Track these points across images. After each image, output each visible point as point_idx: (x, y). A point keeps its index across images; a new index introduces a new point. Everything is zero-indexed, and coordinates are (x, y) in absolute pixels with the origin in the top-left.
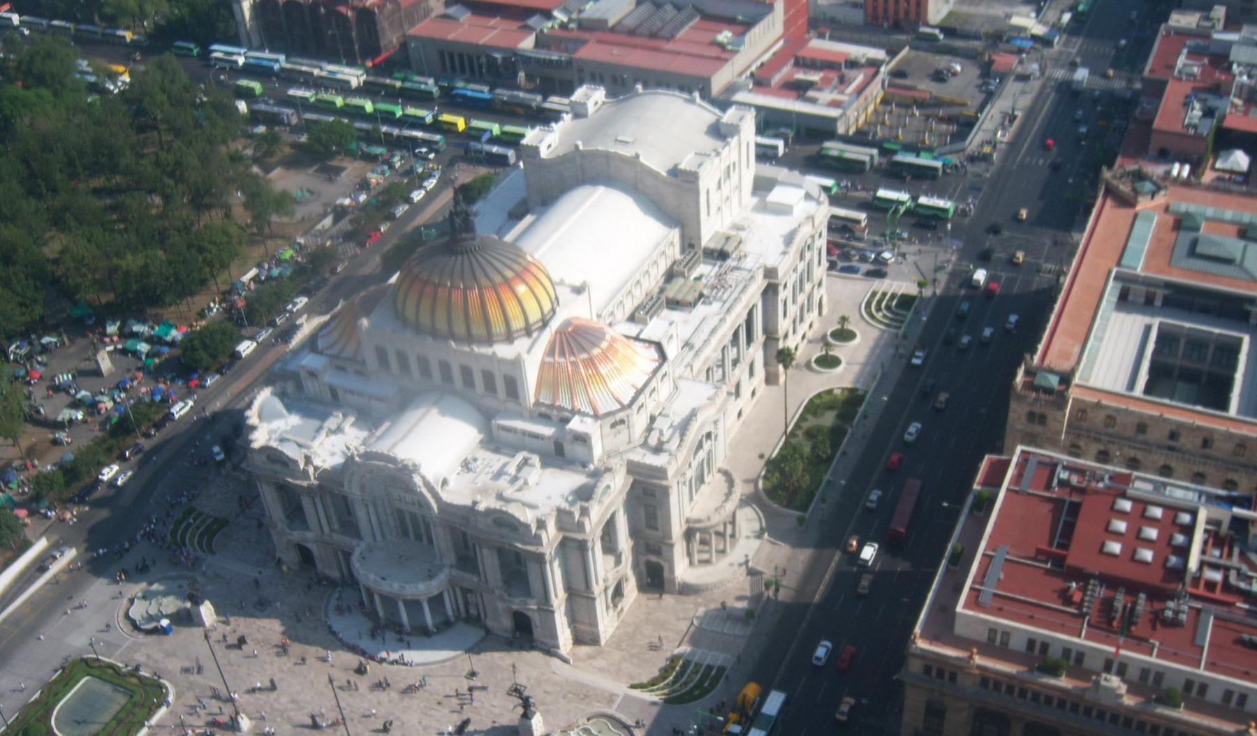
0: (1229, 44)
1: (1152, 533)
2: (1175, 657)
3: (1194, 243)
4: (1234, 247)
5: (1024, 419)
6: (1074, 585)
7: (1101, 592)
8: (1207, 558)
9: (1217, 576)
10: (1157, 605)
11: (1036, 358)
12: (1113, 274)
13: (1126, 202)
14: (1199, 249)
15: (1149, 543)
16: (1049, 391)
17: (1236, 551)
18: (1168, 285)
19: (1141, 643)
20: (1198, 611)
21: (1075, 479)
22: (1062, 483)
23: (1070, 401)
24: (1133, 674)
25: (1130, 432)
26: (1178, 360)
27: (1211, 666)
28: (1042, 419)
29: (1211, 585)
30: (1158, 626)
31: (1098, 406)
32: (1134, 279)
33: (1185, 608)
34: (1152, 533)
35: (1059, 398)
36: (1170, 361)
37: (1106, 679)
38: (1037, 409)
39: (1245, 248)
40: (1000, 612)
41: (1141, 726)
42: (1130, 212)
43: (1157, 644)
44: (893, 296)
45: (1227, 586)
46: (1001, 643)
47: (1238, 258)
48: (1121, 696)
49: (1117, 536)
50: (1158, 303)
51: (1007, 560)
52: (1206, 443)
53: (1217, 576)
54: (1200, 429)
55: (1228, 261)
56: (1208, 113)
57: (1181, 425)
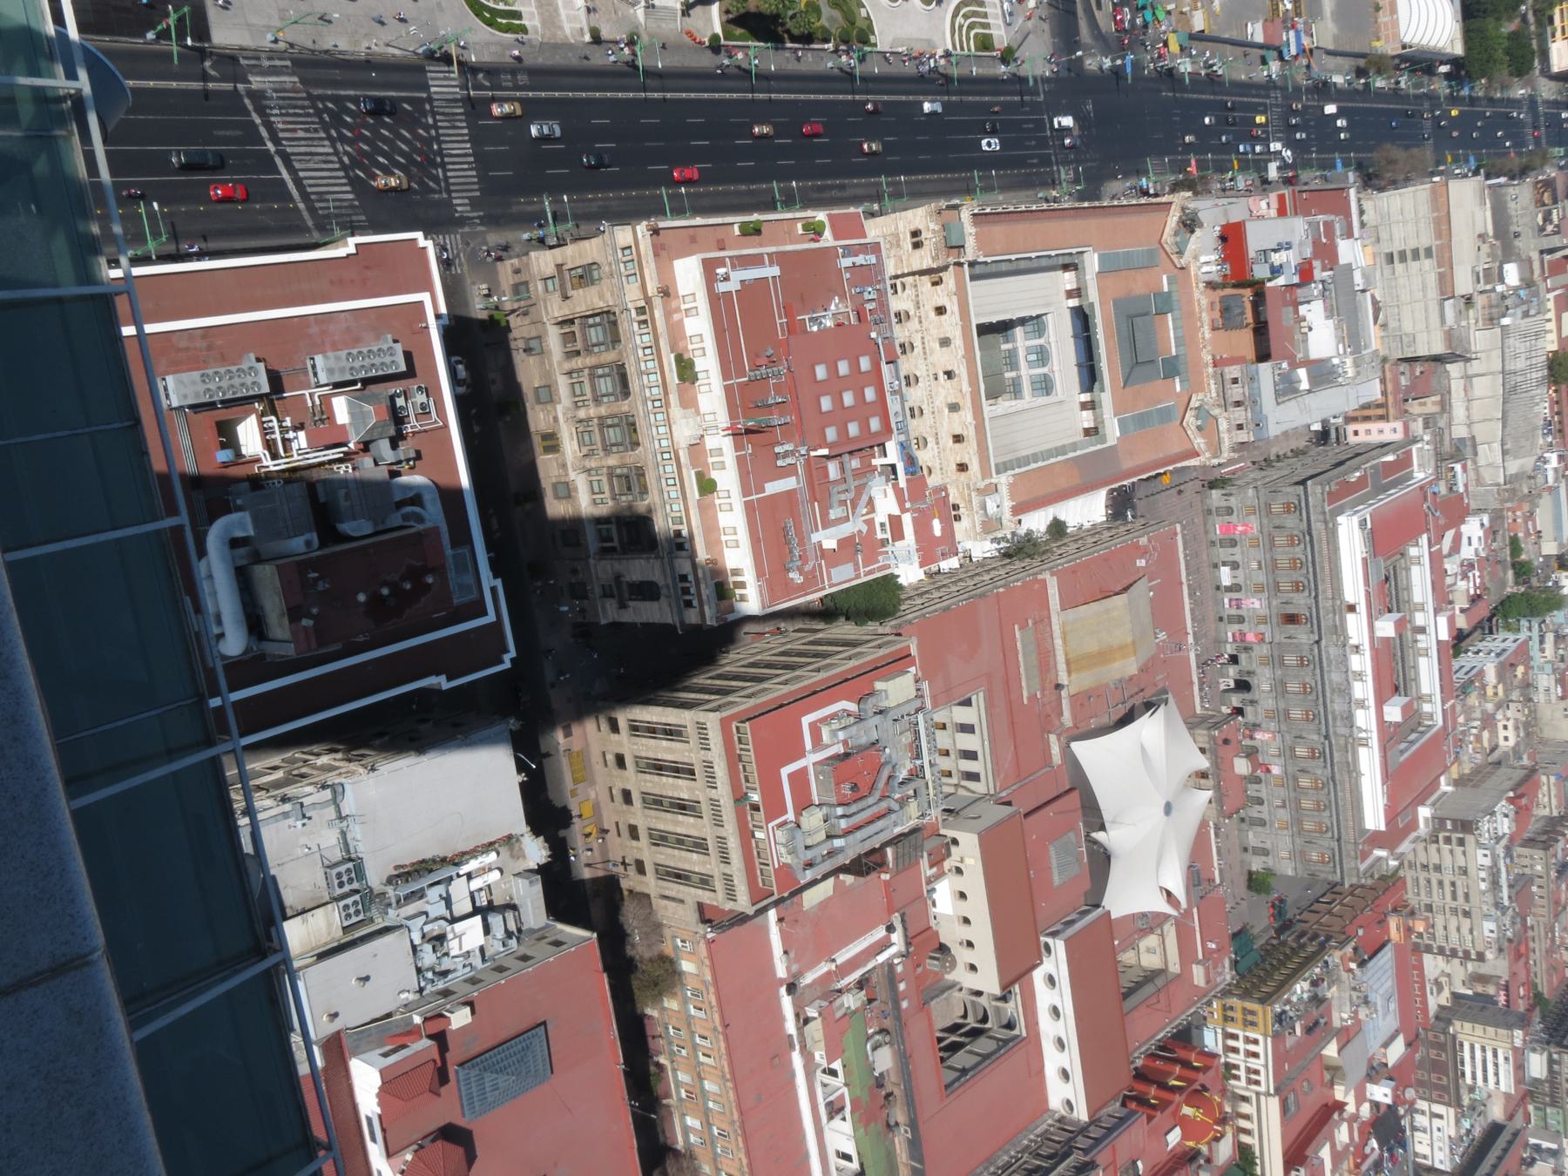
1: (848, 399)
5: (913, 228)
15: (838, 400)
20: (796, 474)
38: (924, 236)
40: (715, 299)
44: (987, 26)
49: (833, 369)
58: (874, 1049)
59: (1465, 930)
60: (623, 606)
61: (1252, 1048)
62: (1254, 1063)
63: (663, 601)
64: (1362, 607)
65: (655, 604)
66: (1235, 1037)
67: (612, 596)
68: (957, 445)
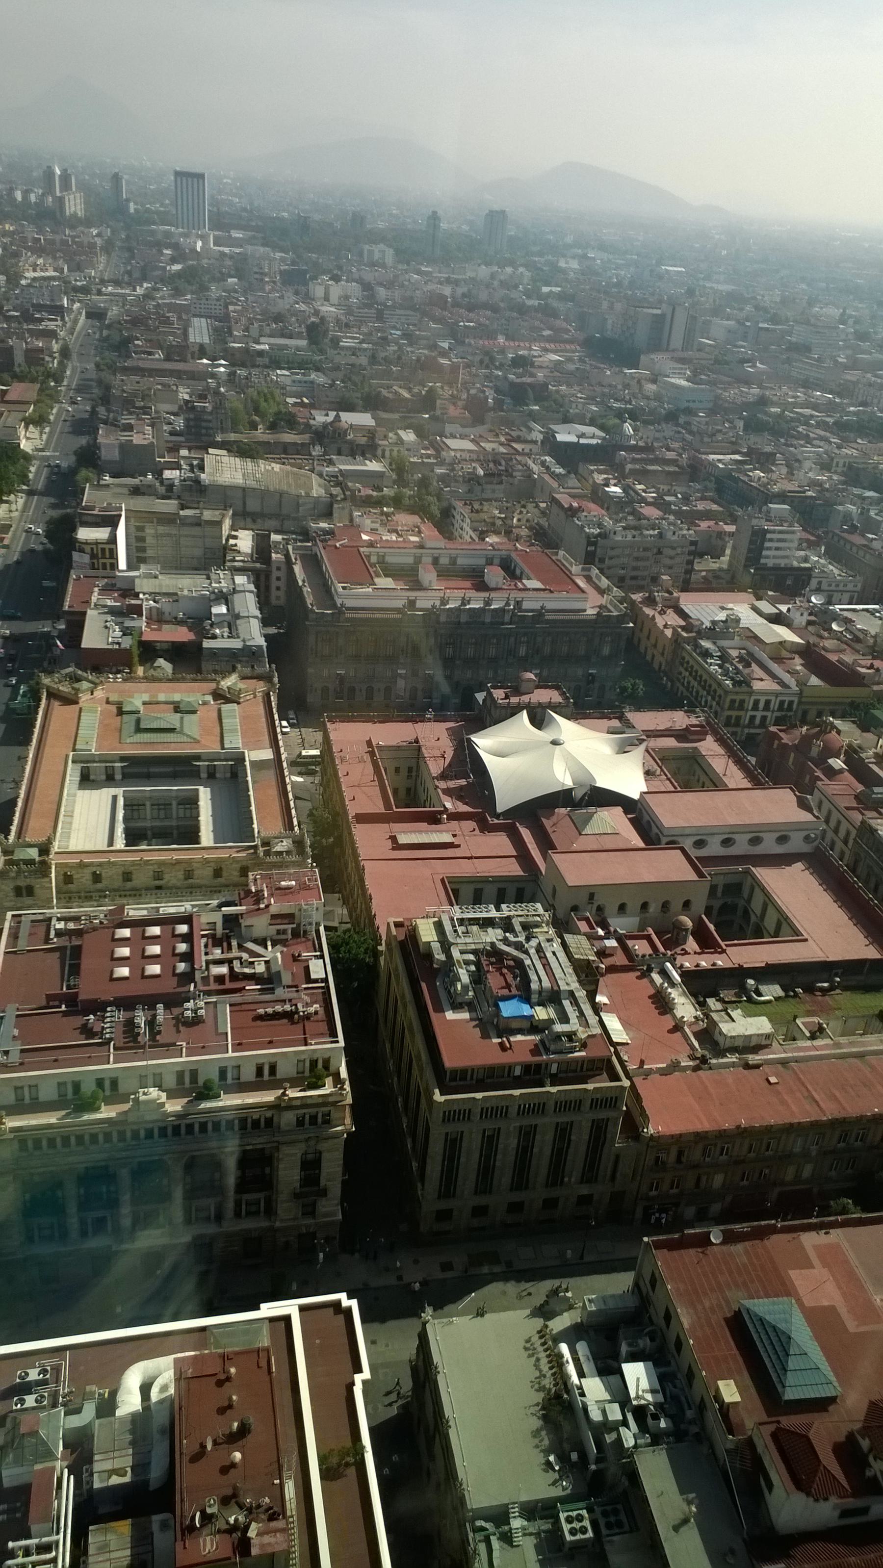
0: (133, 578)
2: (204, 1050)
3: (138, 721)
4: (174, 719)
5: (12, 894)
6: (92, 1017)
7: (121, 1016)
8: (210, 957)
9: (224, 970)
10: (176, 1011)
11: (12, 837)
12: (71, 758)
13: (70, 700)
14: (142, 726)
15: (154, 958)
16: (31, 862)
17: (234, 943)
18: (123, 759)
19: (170, 1048)
21: (71, 926)
22: (59, 933)
23: (53, 867)
24: (170, 1081)
25: (118, 883)
26: (146, 823)
27: (238, 1046)
28: (30, 891)
29: (220, 979)
30: (182, 1028)
31: (82, 865)
32: (91, 759)
33: (201, 1004)
34: (156, 949)
35: (43, 868)
36: (140, 824)
37: (144, 1094)
38: (22, 883)
39: (182, 718)
40: (22, 1066)
41: (190, 1128)
42: (75, 708)
43: (184, 1044)
45: (234, 976)
46: (31, 1099)
47: (177, 725)
48: (163, 1105)
49: (123, 961)
50: (118, 777)
51: (18, 1016)
52: (189, 875)
53: (224, 970)
54: (178, 862)
55: (172, 730)
56: (126, 632)
57: (162, 863)
58: (760, 995)
59: (671, 552)
60: (324, 1193)
61: (761, 705)
62: (774, 705)
63: (323, 1146)
64: (413, 594)
65: (325, 1156)
66: (753, 718)
67: (314, 1204)
68: (224, 874)
